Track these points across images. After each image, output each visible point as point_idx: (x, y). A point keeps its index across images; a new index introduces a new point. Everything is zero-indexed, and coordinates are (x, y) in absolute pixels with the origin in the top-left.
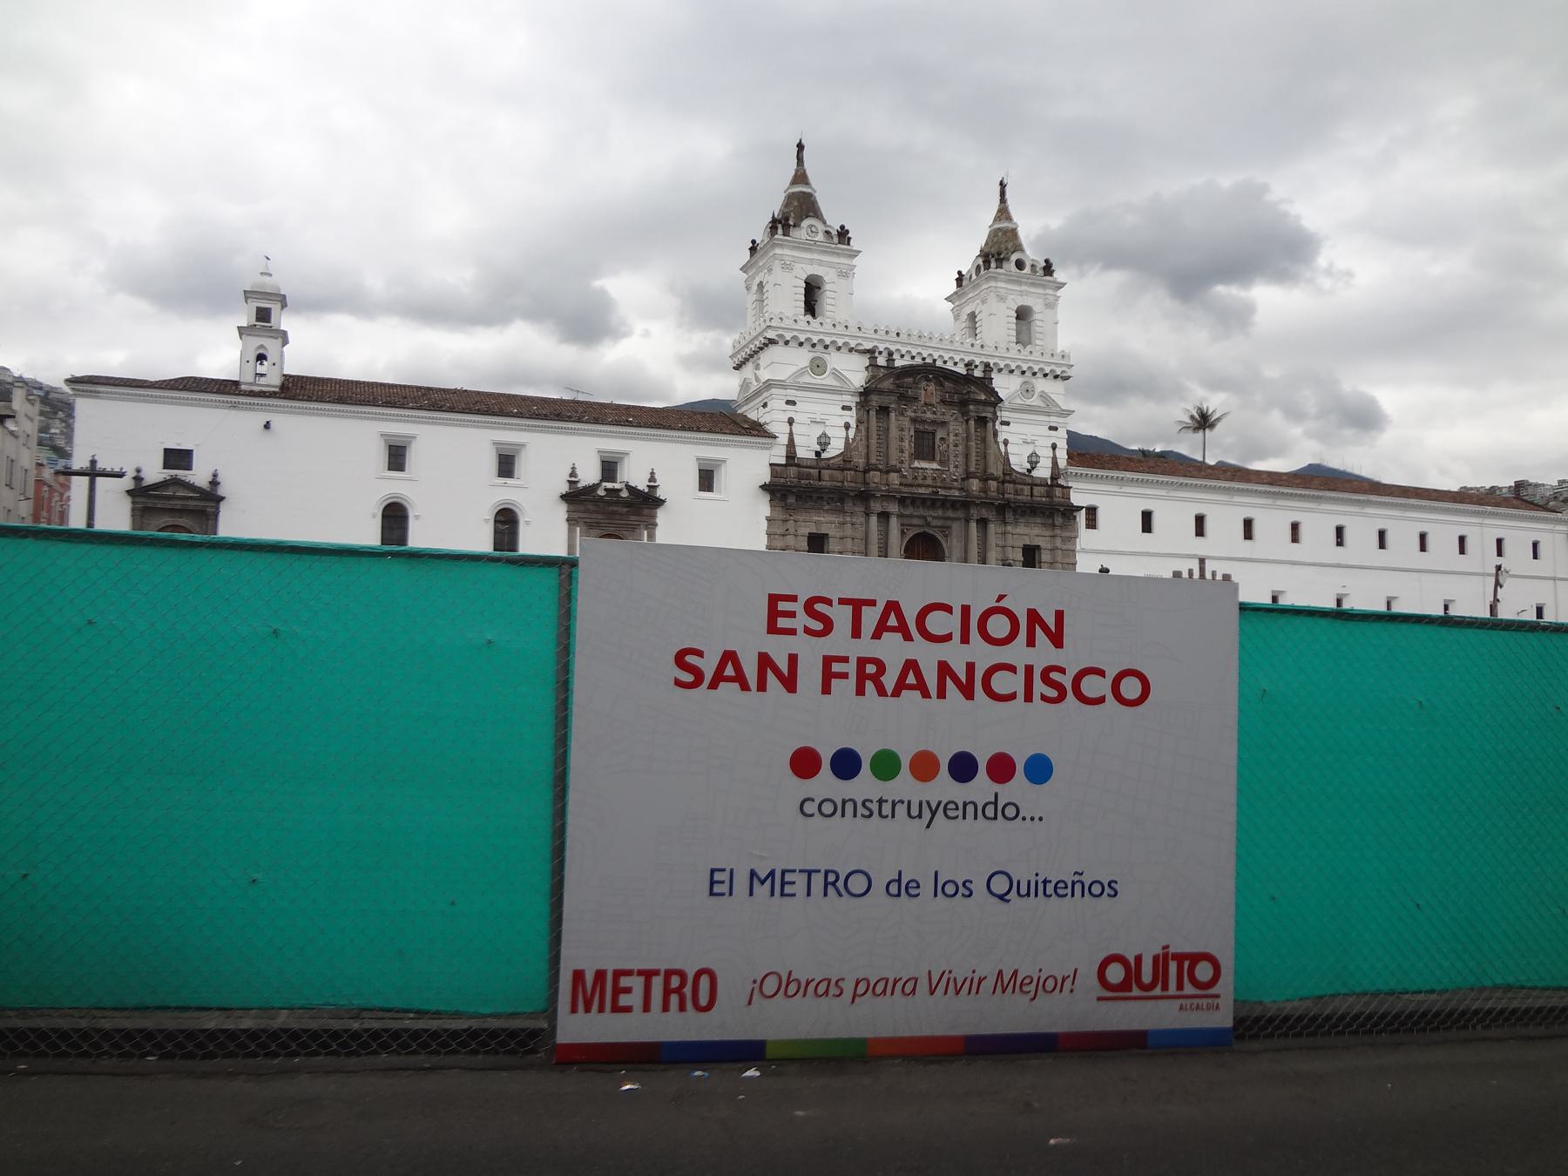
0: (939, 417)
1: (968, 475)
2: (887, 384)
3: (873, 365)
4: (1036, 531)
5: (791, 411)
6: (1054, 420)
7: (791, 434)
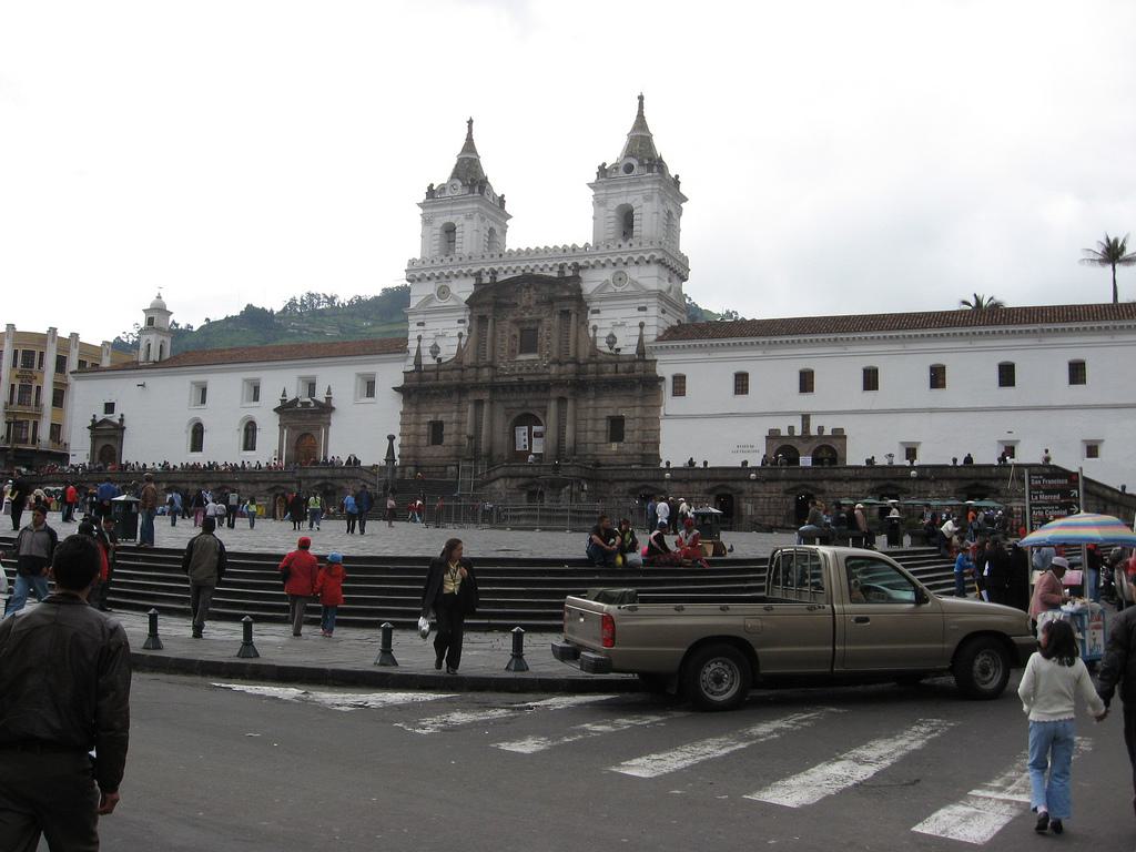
0: (534, 316)
4: (620, 403)
6: (642, 302)
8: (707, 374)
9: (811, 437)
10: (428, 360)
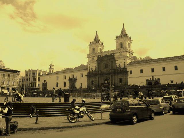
8: (136, 70)
9: (154, 80)
10: (91, 71)
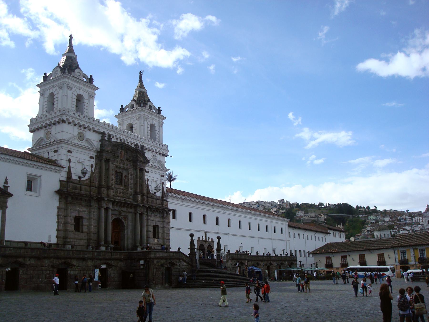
0: (125, 166)
1: (136, 193)
2: (109, 148)
3: (102, 141)
4: (157, 219)
5: (70, 156)
7: (69, 167)
